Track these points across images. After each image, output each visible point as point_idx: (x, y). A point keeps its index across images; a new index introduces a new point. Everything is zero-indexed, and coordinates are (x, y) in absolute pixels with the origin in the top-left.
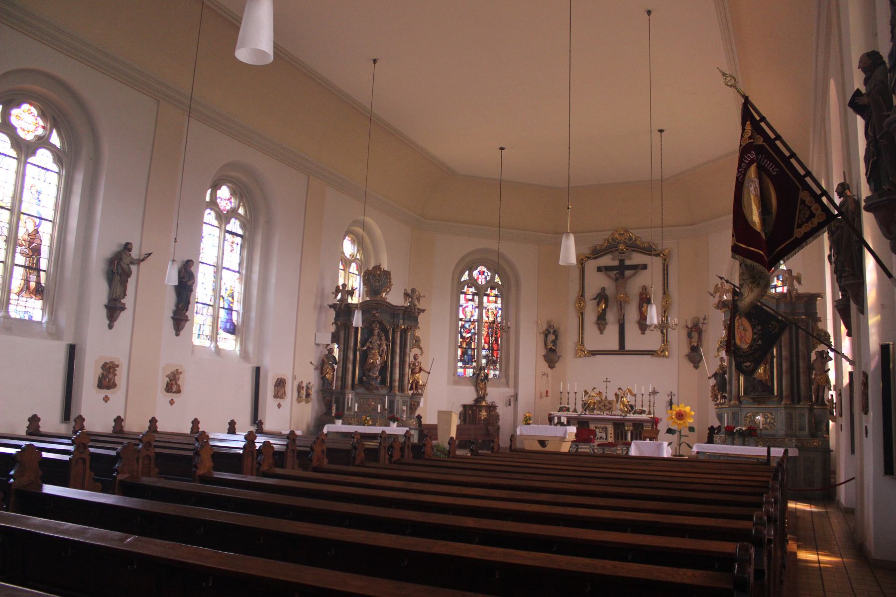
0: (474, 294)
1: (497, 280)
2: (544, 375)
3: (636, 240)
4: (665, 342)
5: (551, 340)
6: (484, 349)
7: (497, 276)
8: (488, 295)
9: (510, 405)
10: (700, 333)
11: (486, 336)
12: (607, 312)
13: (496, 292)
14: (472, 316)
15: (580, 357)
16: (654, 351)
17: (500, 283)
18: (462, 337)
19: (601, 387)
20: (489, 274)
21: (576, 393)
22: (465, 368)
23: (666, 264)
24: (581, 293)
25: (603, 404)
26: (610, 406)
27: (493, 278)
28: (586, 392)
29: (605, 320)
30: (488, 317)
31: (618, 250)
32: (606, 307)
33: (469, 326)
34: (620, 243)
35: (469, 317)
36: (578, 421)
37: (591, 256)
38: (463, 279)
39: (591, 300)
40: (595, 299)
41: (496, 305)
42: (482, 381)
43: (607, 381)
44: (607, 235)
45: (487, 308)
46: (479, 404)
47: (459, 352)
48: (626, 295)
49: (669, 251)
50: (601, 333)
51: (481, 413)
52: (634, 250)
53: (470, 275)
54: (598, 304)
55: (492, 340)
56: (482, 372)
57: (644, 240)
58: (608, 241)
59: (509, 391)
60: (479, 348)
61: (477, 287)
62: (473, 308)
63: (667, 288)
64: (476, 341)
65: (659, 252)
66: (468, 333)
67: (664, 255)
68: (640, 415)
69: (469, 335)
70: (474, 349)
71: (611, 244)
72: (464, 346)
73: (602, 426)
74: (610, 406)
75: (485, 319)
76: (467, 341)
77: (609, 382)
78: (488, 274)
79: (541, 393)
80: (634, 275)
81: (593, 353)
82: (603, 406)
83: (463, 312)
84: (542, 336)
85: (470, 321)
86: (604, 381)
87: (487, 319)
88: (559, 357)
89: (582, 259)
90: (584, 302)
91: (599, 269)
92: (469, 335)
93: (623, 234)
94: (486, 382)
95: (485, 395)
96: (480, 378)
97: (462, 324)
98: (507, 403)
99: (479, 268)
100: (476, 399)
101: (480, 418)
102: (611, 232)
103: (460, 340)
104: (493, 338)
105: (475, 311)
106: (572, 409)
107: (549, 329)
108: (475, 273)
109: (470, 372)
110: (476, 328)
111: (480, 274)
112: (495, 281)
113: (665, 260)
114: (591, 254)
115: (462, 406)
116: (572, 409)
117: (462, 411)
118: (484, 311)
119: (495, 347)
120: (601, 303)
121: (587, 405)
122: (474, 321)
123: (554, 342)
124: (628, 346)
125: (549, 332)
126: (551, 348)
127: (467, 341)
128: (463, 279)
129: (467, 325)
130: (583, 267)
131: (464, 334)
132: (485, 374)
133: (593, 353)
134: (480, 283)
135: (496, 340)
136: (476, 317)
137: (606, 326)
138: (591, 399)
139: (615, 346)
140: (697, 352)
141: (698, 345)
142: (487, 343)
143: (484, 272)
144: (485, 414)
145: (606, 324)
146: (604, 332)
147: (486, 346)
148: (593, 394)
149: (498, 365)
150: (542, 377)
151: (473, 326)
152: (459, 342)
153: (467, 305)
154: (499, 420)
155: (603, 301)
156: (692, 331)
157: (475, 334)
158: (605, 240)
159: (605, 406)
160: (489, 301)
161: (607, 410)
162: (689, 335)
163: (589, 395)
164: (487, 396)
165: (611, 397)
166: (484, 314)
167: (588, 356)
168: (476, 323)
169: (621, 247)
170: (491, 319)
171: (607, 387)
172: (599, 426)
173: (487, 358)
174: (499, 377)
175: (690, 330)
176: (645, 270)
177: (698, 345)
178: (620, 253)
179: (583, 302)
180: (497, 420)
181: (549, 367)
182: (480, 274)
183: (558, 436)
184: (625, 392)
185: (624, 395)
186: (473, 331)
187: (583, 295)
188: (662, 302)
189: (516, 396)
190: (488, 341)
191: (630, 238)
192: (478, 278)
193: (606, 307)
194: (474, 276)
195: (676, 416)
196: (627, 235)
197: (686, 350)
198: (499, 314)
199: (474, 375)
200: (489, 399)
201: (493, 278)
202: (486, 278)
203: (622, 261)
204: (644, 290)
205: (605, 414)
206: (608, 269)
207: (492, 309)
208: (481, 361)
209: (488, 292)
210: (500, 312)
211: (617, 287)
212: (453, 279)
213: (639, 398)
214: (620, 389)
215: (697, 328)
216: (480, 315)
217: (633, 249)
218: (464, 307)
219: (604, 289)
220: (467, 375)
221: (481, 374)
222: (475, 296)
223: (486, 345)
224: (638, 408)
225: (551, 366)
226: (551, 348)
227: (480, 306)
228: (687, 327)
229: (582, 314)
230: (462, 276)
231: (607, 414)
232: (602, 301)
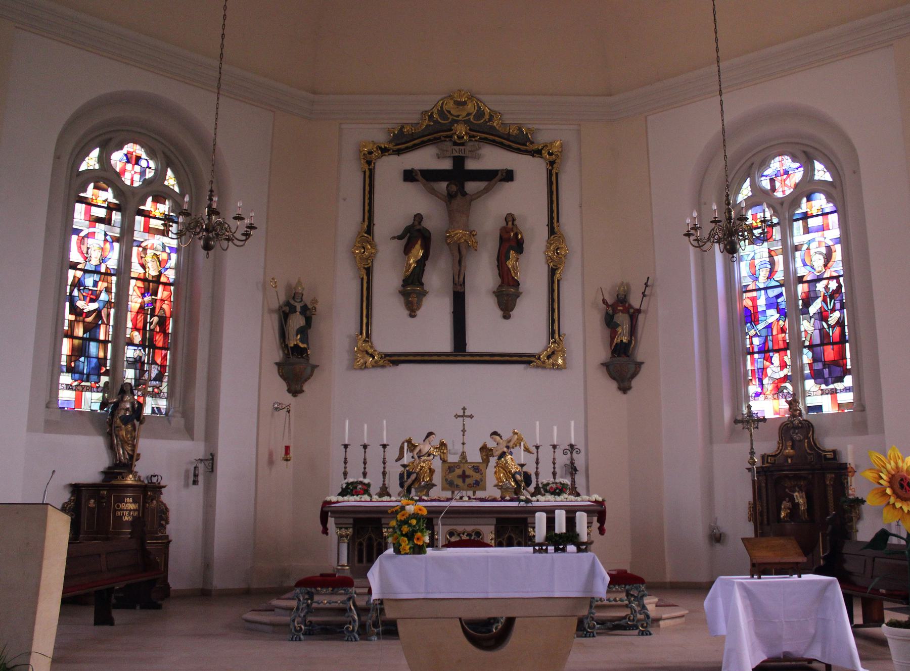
0: (110, 208)
1: (171, 180)
2: (276, 409)
3: (491, 118)
4: (556, 336)
5: (295, 329)
6: (130, 343)
7: (170, 173)
8: (147, 215)
9: (195, 482)
10: (634, 315)
11: (138, 313)
12: (425, 268)
13: (164, 208)
14: (103, 260)
15: (364, 367)
16: (533, 356)
17: (177, 189)
18: (74, 310)
19: (449, 432)
20: (152, 164)
21: (384, 446)
22: (80, 390)
23: (554, 172)
24: (366, 223)
25: (459, 472)
26: (477, 476)
27: (160, 175)
28: (412, 447)
29: (422, 284)
30: (143, 266)
31: (451, 137)
32: (426, 256)
33: (96, 284)
34: (457, 122)
35: (95, 261)
36: (355, 520)
37: (391, 146)
38: (83, 167)
39: (394, 238)
40: (400, 238)
41: (165, 240)
42: (126, 420)
43: (464, 415)
44: (429, 102)
45: (143, 245)
46: (115, 482)
47: (66, 346)
48: (472, 234)
49: (561, 146)
50: (412, 315)
51: (122, 506)
52: (486, 139)
53: (104, 160)
54: (407, 250)
55: (151, 323)
56: (127, 398)
57: (508, 119)
58: (431, 117)
59: (195, 449)
60: (119, 341)
61: (121, 190)
62: (106, 241)
63: (558, 221)
64: (111, 323)
65: (540, 148)
66: (92, 301)
67: (550, 154)
68: (558, 498)
69: (94, 306)
70: (105, 342)
71: (436, 122)
72: (79, 331)
73: (469, 528)
74: (477, 476)
75: (136, 270)
76: (90, 319)
77: (471, 417)
78: (150, 166)
79: (271, 455)
80: (486, 190)
81: (395, 359)
82: (459, 476)
83: (79, 248)
84: (275, 317)
85: (96, 272)
86: (457, 416)
87: (142, 271)
88: (314, 367)
89: (370, 153)
90: (374, 246)
91: (409, 176)
92: (94, 306)
93: (465, 103)
94: (137, 423)
95: (133, 457)
96: (122, 413)
97: (75, 277)
98: (187, 477)
99: (129, 147)
100: (109, 468)
101: (121, 517)
102: (439, 97)
103: (69, 317)
104: (156, 319)
105: (112, 248)
106: (375, 489)
107: (292, 302)
108: (117, 158)
109: (92, 400)
110: (114, 290)
111: (128, 161)
112: (166, 183)
113: (552, 163)
114: (390, 142)
115: (71, 489)
116: (375, 489)
117: (70, 500)
118: (135, 250)
119: (159, 340)
120: (413, 246)
121: (413, 477)
122: (108, 274)
123: (303, 332)
124: (473, 345)
125: (293, 310)
126: (296, 346)
127: (90, 319)
128: (83, 167)
129: (89, 281)
130: (370, 170)
131: (80, 304)
132: (133, 405)
133: (395, 359)
134: (128, 183)
135: (163, 322)
136: (113, 263)
137: (424, 299)
138: (424, 462)
139: (445, 345)
140: (628, 356)
141: (630, 342)
142: (138, 330)
143: (138, 158)
144: (132, 506)
145: (424, 293)
146: (418, 313)
147: (137, 338)
148: (426, 448)
150: (272, 415)
151: (105, 285)
152: (66, 323)
153: (92, 230)
154: (167, 523)
155: (419, 242)
156: (615, 311)
157: (108, 304)
158: (424, 113)
159: (464, 476)
160: (147, 229)
161: (470, 487)
162: (610, 322)
163: (417, 450)
164: (137, 460)
165: (475, 457)
166: (135, 259)
167: (383, 366)
168: (114, 279)
169: (461, 129)
170: (153, 272)
171: (464, 431)
172: (460, 528)
173: (138, 365)
174: (167, 414)
175: (610, 310)
176: (510, 183)
177: (630, 342)
178: (455, 144)
179: (370, 244)
180: (163, 522)
181: (289, 391)
182: (128, 161)
183: (557, 594)
184: (509, 441)
185: (508, 447)
186: (104, 297)
187: (369, 230)
188: (548, 248)
189: (210, 462)
190: (140, 325)
191: (480, 114)
192: (124, 170)
193: (426, 256)
194: (113, 162)
195: (894, 492)
196: (471, 107)
197: (601, 352)
198: (172, 263)
199: (103, 405)
200: (143, 469)
201: (160, 175)
202: (143, 173)
203: (459, 161)
204: (510, 223)
205: (466, 498)
206: (430, 176)
207: (156, 249)
208: (123, 373)
209: (149, 205)
210: (174, 256)
211: (451, 214)
212: (57, 157)
213: (546, 455)
214: (495, 433)
215: (627, 305)
216: (125, 259)
217: (484, 136)
218: (82, 234)
219: (418, 218)
220: (85, 407)
221: (122, 405)
222: (114, 212)
223: (136, 333)
224: (546, 478)
225: (295, 390)
226: (296, 346)
227: (126, 238)
228: (604, 301)
229: (369, 271)
230: (84, 160)
231: (470, 498)
232: (416, 243)
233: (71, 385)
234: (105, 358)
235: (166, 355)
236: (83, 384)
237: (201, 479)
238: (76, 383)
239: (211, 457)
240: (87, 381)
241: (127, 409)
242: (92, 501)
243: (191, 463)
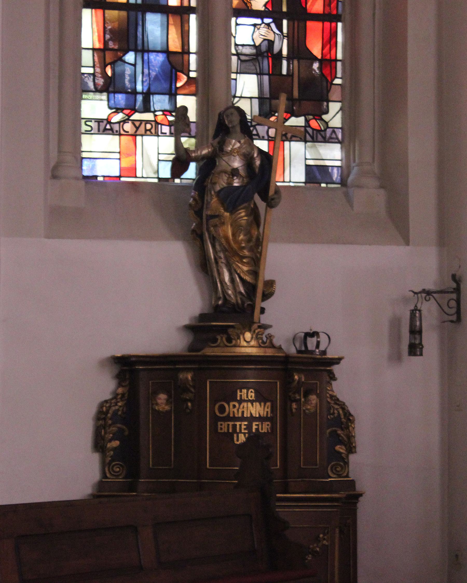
46: (209, 351)
94: (261, 205)
96: (222, 182)
100: (202, 317)
101: (229, 436)
115: (115, 369)
117: (115, 396)
149: (334, 107)
154: (351, 449)
164: (266, 296)
173: (266, 64)
174: (343, 182)
180: (340, 449)
233: (109, 121)
234: (186, 52)
235: (334, 34)
236: (137, 116)
237: (300, 355)
238: (119, 117)
239: (454, 285)
240: (146, 108)
241: (234, 172)
242: (162, 397)
243: (406, 300)
